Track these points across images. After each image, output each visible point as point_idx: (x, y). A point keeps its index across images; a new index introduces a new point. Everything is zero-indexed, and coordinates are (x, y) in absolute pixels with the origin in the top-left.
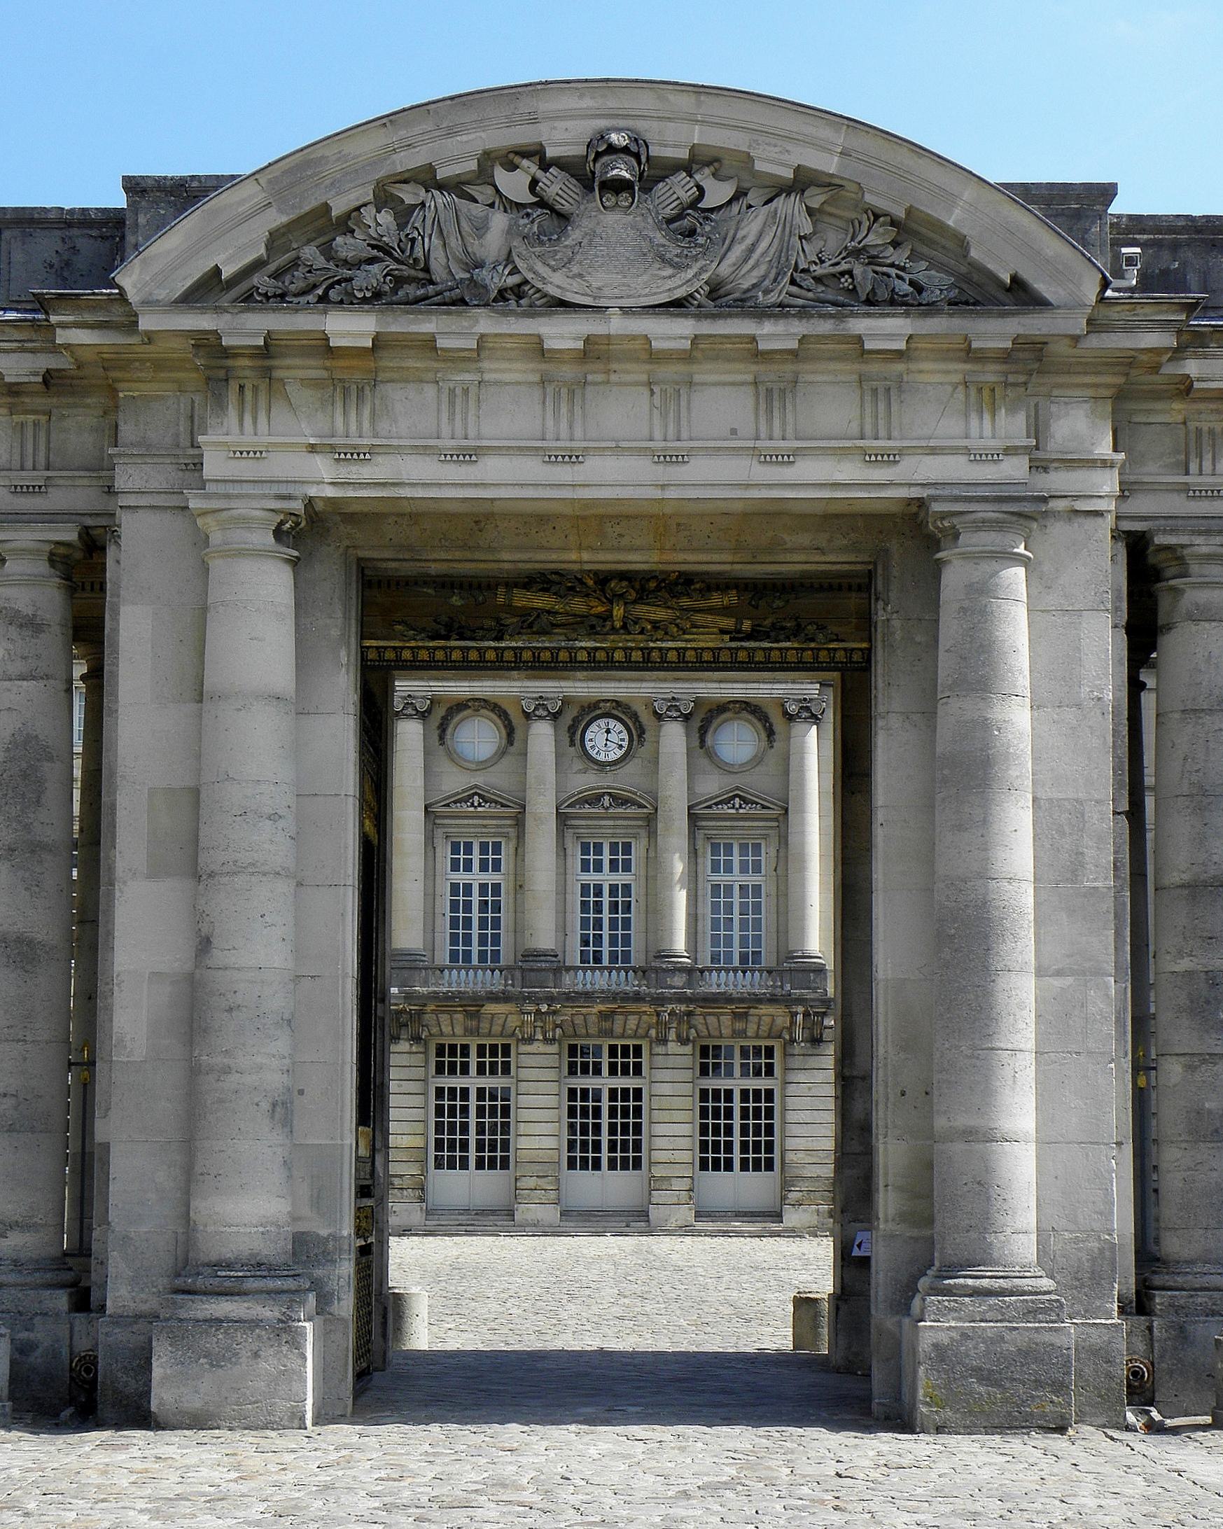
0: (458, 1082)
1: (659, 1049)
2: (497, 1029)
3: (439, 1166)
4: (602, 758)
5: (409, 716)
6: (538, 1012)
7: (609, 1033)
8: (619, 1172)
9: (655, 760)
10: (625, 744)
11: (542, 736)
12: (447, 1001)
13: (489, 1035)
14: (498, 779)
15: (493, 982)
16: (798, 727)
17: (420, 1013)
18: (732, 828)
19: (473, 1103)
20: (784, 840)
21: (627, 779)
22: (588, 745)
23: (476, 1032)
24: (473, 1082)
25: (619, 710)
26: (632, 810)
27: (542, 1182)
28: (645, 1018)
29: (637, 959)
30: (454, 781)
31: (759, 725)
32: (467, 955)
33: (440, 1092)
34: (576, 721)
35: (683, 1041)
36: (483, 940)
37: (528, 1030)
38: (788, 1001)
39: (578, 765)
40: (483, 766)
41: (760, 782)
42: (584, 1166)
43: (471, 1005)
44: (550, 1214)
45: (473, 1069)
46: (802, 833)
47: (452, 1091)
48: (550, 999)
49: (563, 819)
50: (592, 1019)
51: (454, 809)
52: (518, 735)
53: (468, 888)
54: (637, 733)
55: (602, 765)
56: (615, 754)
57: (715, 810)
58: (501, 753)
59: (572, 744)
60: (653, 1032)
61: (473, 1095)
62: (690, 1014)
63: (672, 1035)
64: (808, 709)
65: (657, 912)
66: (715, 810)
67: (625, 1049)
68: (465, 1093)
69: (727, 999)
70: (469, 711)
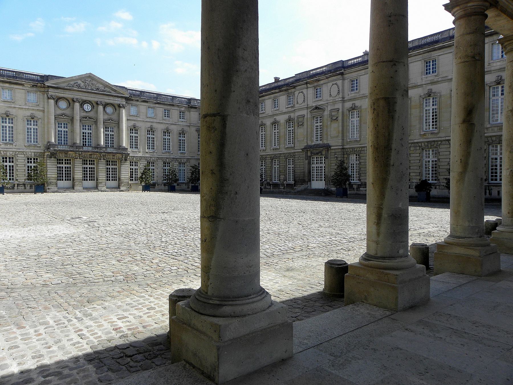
1: (99, 161)
2: (70, 156)
7: (91, 158)
8: (91, 181)
9: (97, 112)
12: (61, 151)
13: (69, 157)
14: (68, 112)
16: (121, 109)
17: (56, 153)
18: (109, 124)
20: (119, 127)
21: (91, 114)
22: (84, 108)
23: (65, 157)
24: (64, 166)
25: (89, 102)
28: (97, 155)
29: (93, 145)
30: (59, 112)
31: (114, 108)
32: (61, 143)
35: (104, 160)
37: (77, 157)
38: (122, 154)
39: (82, 111)
40: (64, 109)
41: (114, 117)
43: (66, 152)
44: (81, 188)
45: (64, 163)
46: (123, 126)
47: (60, 167)
48: (82, 152)
50: (88, 155)
51: (59, 117)
52: (71, 104)
54: (93, 107)
57: (107, 121)
58: (67, 108)
59: (81, 107)
60: (99, 158)
62: (105, 155)
63: (102, 158)
64: (123, 106)
65: (98, 137)
66: (107, 121)
67: (92, 160)
68: (62, 167)
69: (113, 153)
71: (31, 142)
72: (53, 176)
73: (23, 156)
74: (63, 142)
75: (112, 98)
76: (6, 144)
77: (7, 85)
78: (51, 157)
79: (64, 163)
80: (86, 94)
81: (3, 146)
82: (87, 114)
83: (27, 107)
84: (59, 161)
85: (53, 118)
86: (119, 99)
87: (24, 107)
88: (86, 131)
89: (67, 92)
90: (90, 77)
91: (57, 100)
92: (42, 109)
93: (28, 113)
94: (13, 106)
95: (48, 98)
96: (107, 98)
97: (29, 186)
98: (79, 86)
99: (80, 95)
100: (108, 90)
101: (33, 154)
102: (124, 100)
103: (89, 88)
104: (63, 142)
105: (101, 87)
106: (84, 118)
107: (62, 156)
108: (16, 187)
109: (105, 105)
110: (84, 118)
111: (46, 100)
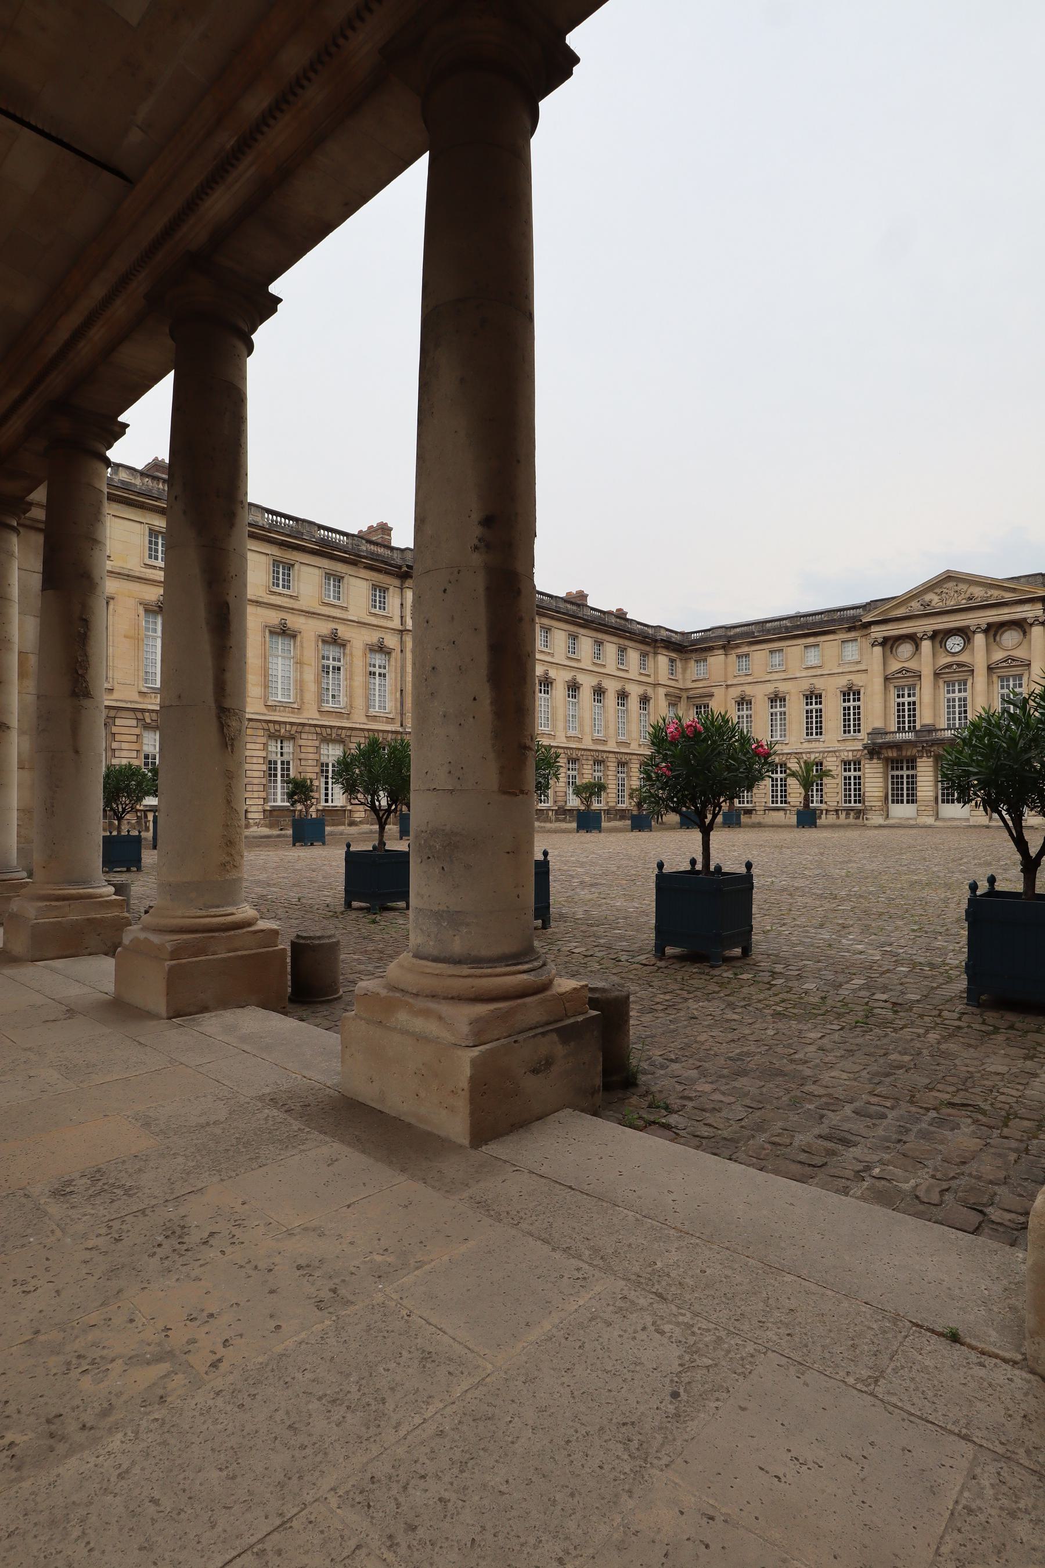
0: (899, 773)
3: (893, 802)
4: (953, 651)
5: (876, 645)
6: (923, 747)
10: (962, 645)
11: (926, 645)
15: (910, 736)
19: (905, 780)
21: (963, 658)
24: (905, 773)
26: (966, 669)
27: (927, 808)
30: (895, 666)
31: (1019, 630)
32: (904, 728)
33: (893, 777)
34: (942, 639)
36: (909, 722)
42: (948, 802)
43: (898, 746)
45: (905, 768)
47: (897, 776)
48: (927, 741)
49: (937, 675)
53: (903, 704)
55: (954, 654)
56: (957, 649)
57: (1000, 665)
61: (905, 777)
68: (902, 777)
70: (901, 641)
71: (849, 732)
72: (876, 794)
73: (835, 759)
74: (907, 725)
75: (1006, 610)
76: (809, 741)
77: (811, 640)
78: (871, 759)
79: (905, 768)
80: (945, 618)
81: (806, 745)
82: (956, 659)
83: (840, 671)
84: (894, 763)
85: (878, 682)
86: (1027, 607)
87: (836, 671)
88: (954, 695)
89: (906, 624)
90: (949, 578)
91: (889, 644)
92: (864, 668)
93: (842, 682)
94: (819, 673)
95: (873, 645)
96: (994, 612)
97: (844, 813)
98: (928, 605)
99: (932, 622)
100: (996, 593)
101: (850, 753)
102: (1039, 606)
103: (952, 603)
104: (907, 725)
105: (978, 592)
106: (946, 667)
107: (892, 754)
108: (823, 816)
109: (993, 630)
110: (946, 667)
111: (869, 649)
